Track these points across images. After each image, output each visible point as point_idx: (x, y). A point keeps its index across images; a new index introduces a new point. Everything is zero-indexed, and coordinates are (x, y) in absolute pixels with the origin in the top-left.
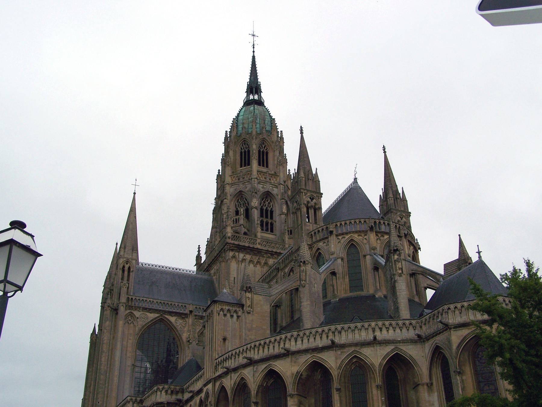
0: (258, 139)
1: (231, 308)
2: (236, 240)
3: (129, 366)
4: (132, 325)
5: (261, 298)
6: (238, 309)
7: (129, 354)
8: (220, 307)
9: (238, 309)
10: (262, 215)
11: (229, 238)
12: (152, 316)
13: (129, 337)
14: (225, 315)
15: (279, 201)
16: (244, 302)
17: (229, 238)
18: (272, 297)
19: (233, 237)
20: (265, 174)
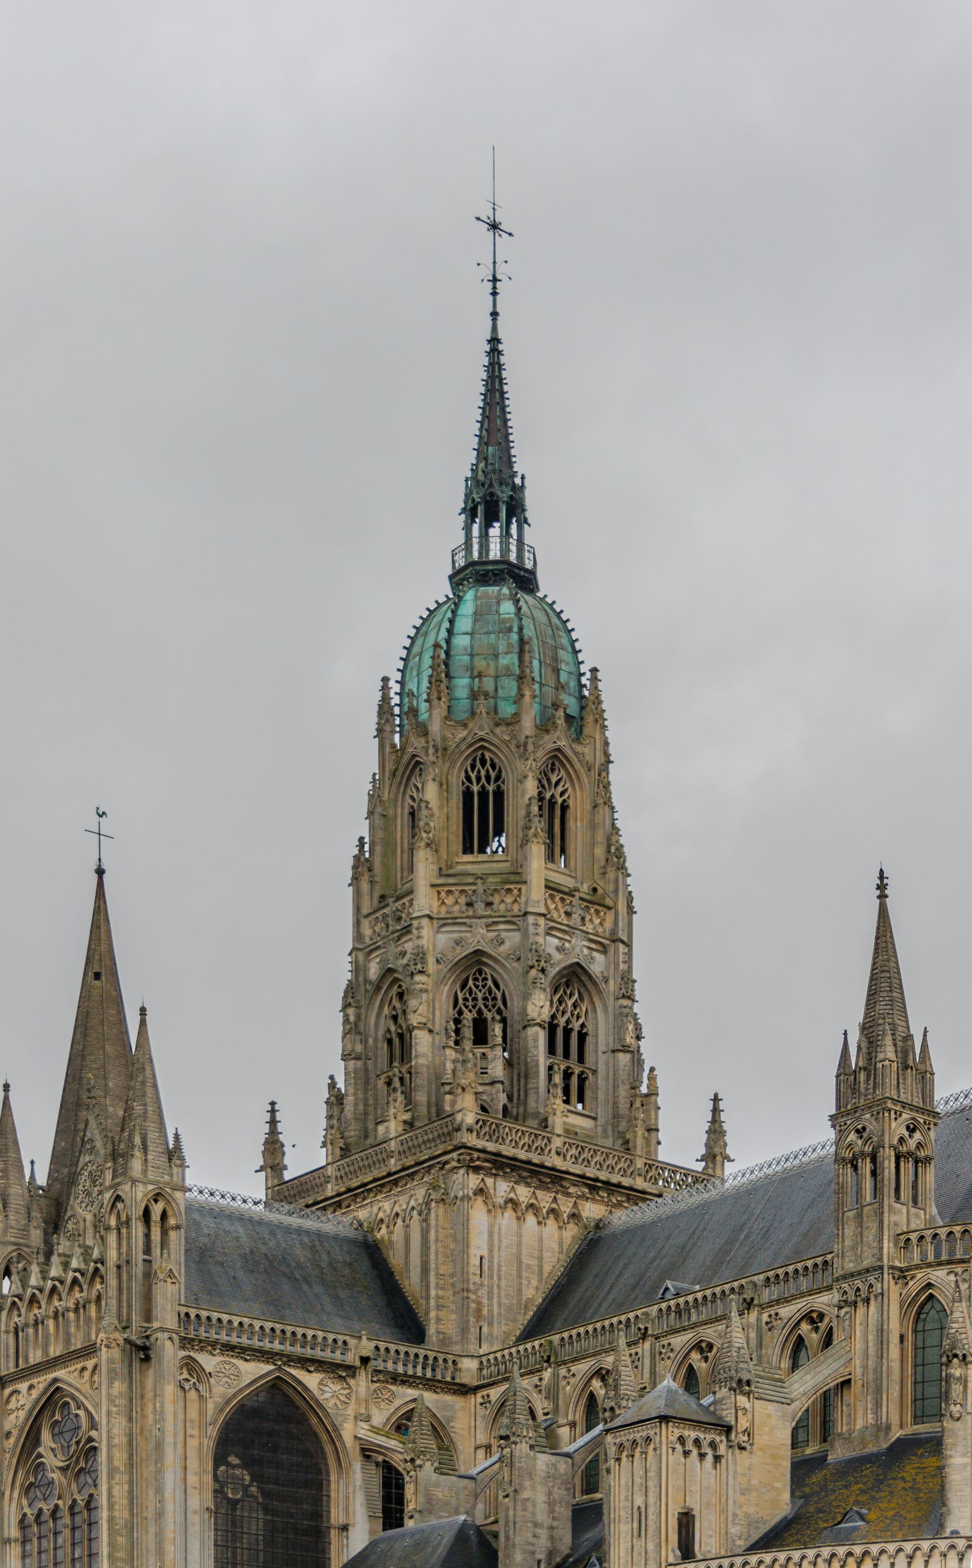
0: (540, 753)
1: (702, 1436)
2: (490, 1140)
3: (195, 1512)
4: (193, 1391)
5: (771, 1407)
6: (718, 1439)
7: (192, 1480)
8: (676, 1431)
9: (718, 1439)
10: (551, 1050)
11: (470, 1130)
12: (253, 1370)
13: (189, 1431)
14: (686, 1454)
15: (610, 1002)
16: (731, 1420)
17: (470, 1130)
18: (793, 1406)
19: (479, 1127)
20: (568, 899)
